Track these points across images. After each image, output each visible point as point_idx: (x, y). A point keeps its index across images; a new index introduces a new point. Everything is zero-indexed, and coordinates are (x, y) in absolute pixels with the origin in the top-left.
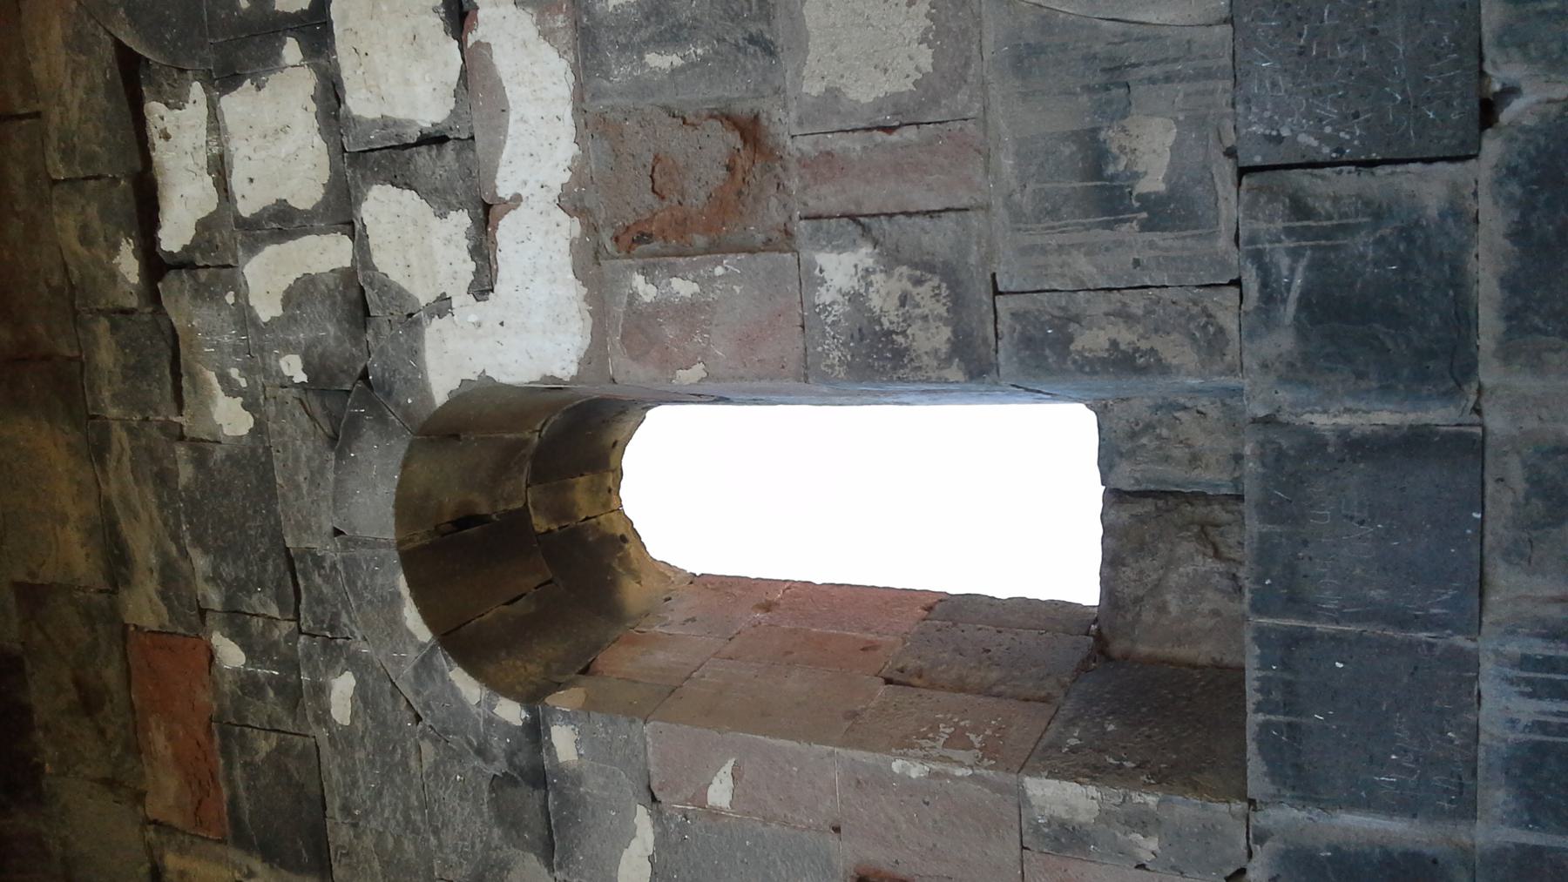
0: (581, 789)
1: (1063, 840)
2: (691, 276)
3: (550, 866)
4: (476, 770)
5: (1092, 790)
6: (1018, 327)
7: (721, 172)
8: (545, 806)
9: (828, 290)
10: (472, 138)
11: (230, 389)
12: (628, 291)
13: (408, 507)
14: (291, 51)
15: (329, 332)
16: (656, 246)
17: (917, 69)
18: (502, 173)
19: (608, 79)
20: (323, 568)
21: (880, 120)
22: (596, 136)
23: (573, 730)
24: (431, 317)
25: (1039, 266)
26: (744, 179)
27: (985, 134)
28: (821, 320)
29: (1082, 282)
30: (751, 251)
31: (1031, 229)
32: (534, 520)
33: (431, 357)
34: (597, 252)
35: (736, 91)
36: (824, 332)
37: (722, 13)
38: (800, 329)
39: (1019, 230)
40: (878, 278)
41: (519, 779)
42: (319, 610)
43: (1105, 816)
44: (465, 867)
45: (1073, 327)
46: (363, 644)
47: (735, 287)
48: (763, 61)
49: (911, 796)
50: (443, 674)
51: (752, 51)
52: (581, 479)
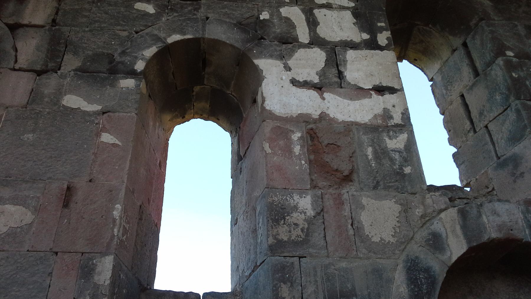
0: (108, 87)
1: (86, 269)
2: (301, 152)
3: (76, 70)
4: (116, 50)
5: (108, 282)
6: (288, 264)
7: (335, 167)
8: (100, 72)
9: (298, 199)
10: (341, 88)
12: (295, 130)
13: (216, 44)
15: (278, 29)
16: (310, 142)
17: (372, 236)
18: (332, 95)
19: (363, 134)
20: (194, 11)
21: (355, 222)
22: (345, 128)
23: (133, 87)
24: (284, 64)
25: (310, 273)
26: (333, 174)
27: (352, 258)
28: (287, 195)
29: (305, 288)
31: (322, 272)
32: (198, 87)
33: (270, 61)
34: (307, 122)
36: (284, 196)
37: (385, 173)
38: (284, 188)
39: (322, 267)
40: (303, 216)
41: (113, 65)
42: (179, 6)
43: (97, 286)
44: (76, 39)
45: (289, 284)
46: (166, 19)
47: (298, 167)
48: (372, 185)
49: (105, 211)
50: (155, 44)
51: (374, 182)
52: (208, 106)
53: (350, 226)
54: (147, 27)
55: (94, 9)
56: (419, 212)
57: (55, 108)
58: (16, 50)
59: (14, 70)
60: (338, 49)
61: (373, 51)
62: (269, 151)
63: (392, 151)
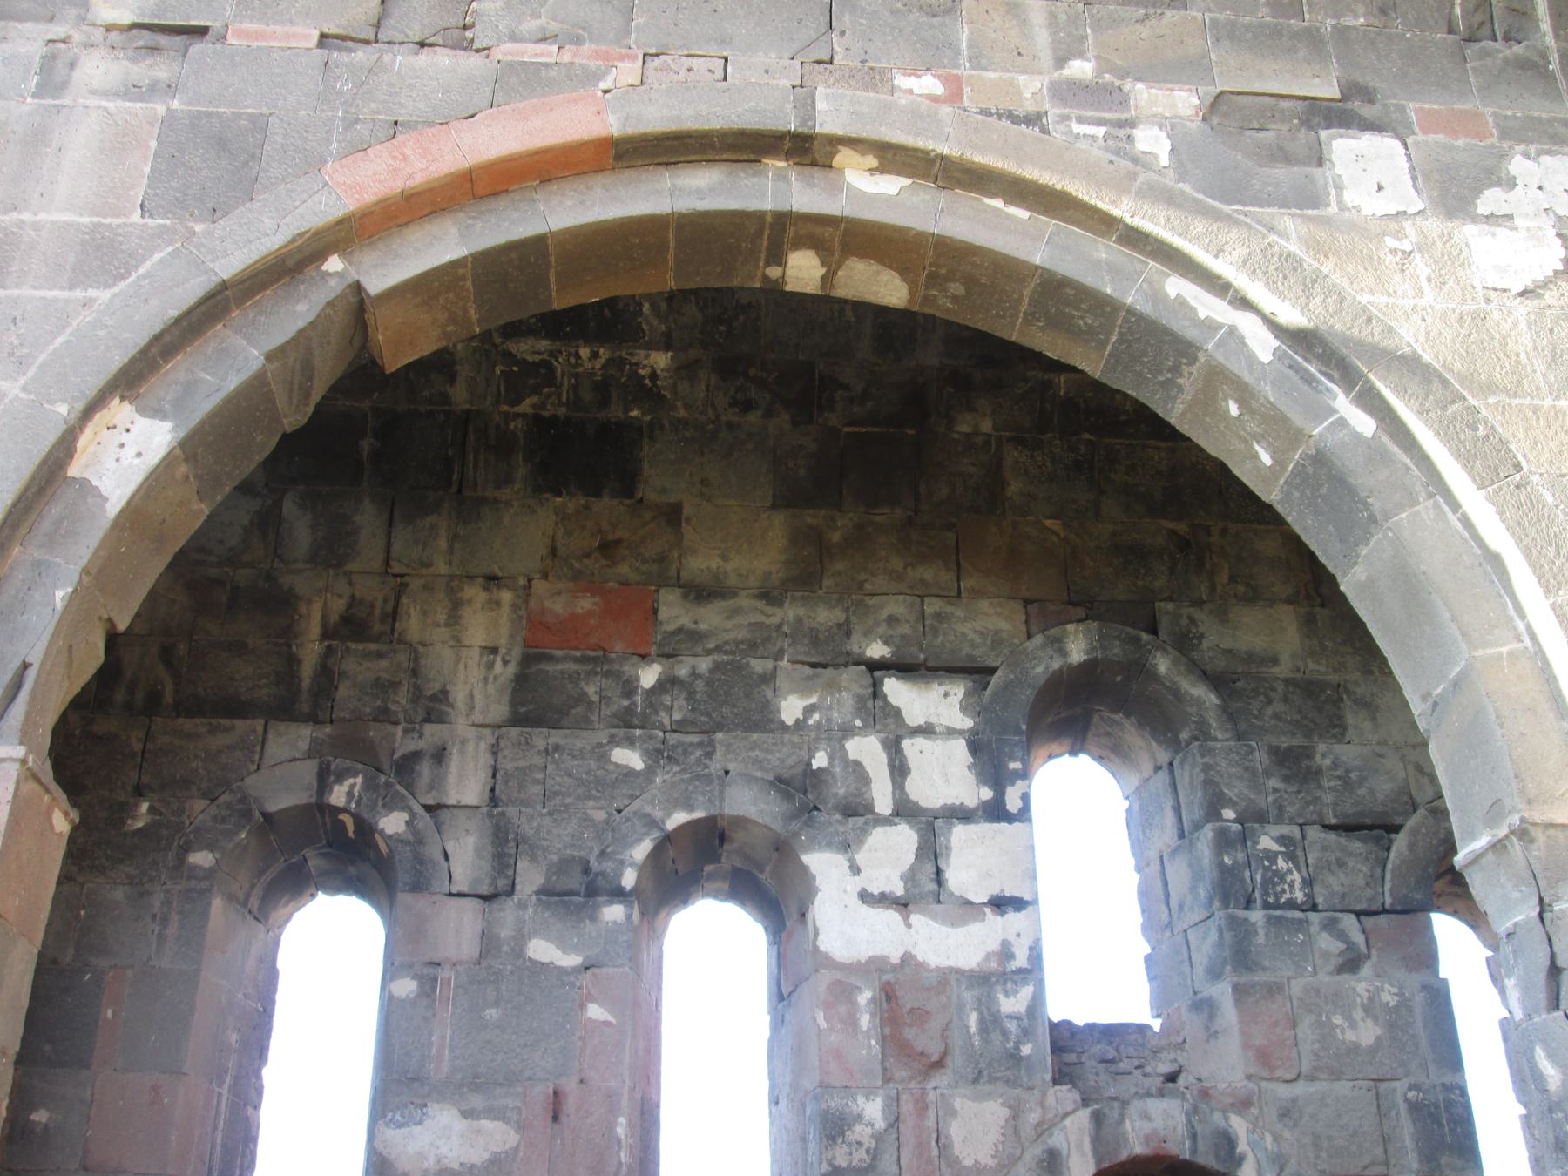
3: (538, 893)
4: (591, 849)
10: (939, 902)
11: (809, 710)
13: (740, 822)
14: (987, 794)
15: (840, 789)
16: (885, 1005)
18: (922, 918)
30: (883, 1062)
35: (956, 1060)
40: (869, 1130)
48: (970, 1077)
50: (647, 834)
53: (934, 1143)
54: (633, 798)
55: (550, 768)
56: (1033, 1117)
57: (519, 962)
58: (446, 857)
59: (451, 894)
60: (939, 823)
61: (996, 826)
62: (823, 1024)
63: (1007, 1017)
